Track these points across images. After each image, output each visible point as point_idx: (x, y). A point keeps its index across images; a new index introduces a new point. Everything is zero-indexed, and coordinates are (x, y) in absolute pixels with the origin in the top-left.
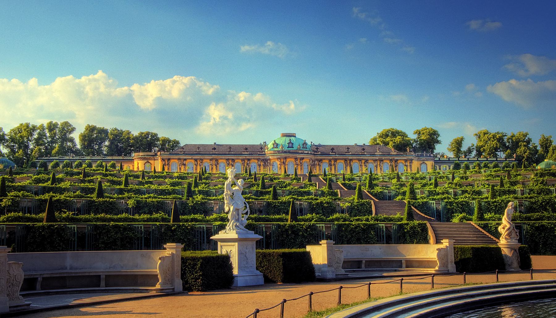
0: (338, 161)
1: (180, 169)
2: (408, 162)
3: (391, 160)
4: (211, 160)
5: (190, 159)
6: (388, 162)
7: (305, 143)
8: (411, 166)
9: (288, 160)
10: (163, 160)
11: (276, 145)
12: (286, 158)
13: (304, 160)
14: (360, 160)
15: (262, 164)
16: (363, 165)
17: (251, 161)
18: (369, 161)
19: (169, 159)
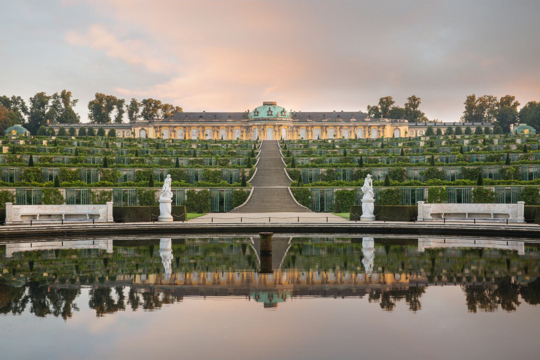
0: (315, 128)
1: (171, 135)
2: (381, 128)
3: (365, 127)
4: (198, 127)
5: (179, 126)
6: (362, 128)
7: (283, 111)
8: (383, 131)
9: (267, 127)
10: (155, 127)
11: (256, 112)
12: (265, 125)
13: (282, 127)
14: (335, 126)
15: (244, 130)
16: (338, 130)
17: (234, 128)
18: (344, 127)
19: (160, 127)
